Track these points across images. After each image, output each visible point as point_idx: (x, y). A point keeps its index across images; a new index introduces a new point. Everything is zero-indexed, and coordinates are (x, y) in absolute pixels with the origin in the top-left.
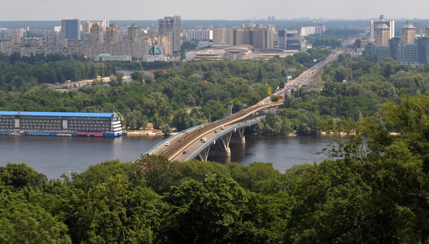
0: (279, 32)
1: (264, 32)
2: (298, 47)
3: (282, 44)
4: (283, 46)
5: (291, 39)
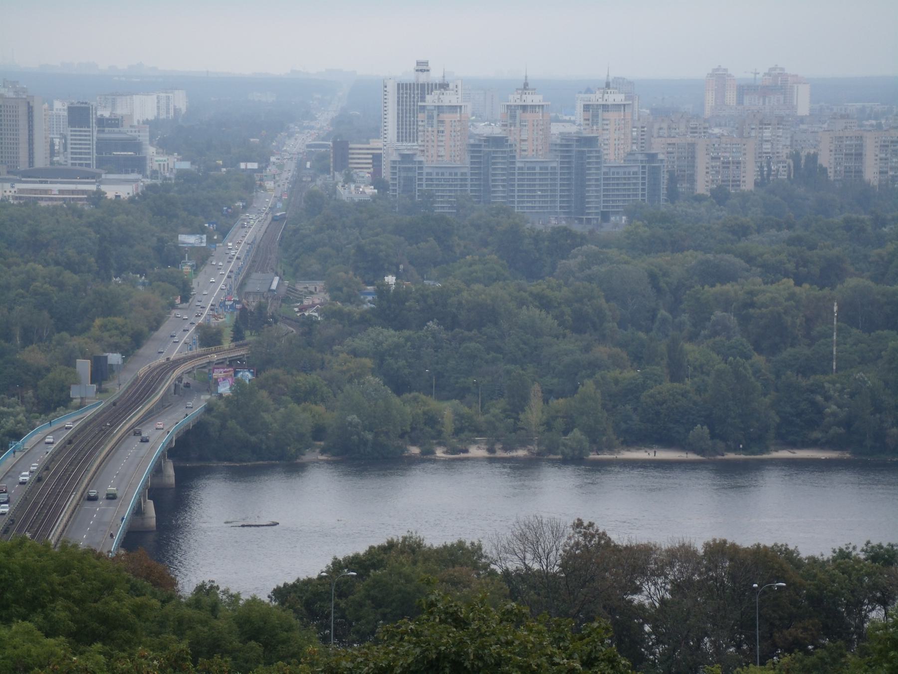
0: (71, 110)
1: (23, 110)
2: (137, 164)
3: (80, 153)
4: (86, 159)
5: (110, 134)
